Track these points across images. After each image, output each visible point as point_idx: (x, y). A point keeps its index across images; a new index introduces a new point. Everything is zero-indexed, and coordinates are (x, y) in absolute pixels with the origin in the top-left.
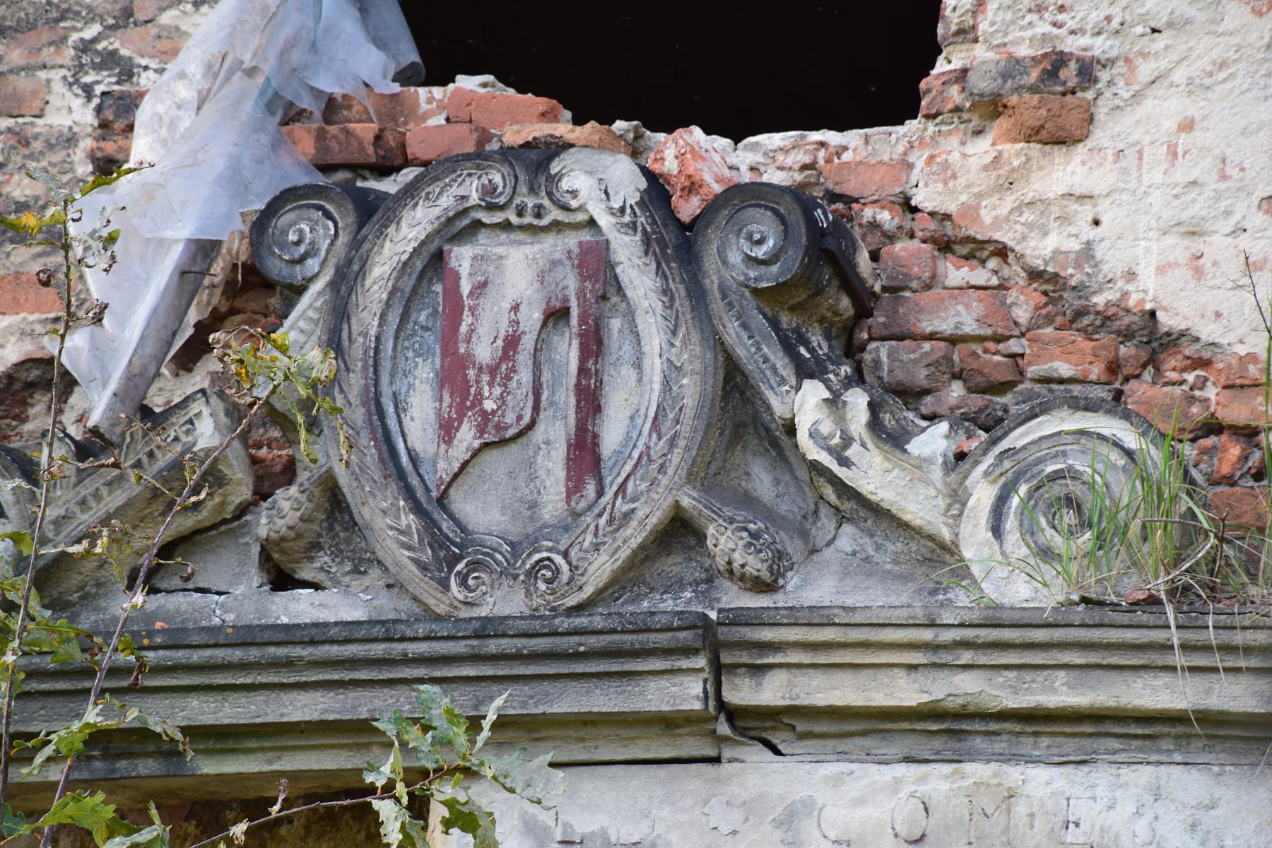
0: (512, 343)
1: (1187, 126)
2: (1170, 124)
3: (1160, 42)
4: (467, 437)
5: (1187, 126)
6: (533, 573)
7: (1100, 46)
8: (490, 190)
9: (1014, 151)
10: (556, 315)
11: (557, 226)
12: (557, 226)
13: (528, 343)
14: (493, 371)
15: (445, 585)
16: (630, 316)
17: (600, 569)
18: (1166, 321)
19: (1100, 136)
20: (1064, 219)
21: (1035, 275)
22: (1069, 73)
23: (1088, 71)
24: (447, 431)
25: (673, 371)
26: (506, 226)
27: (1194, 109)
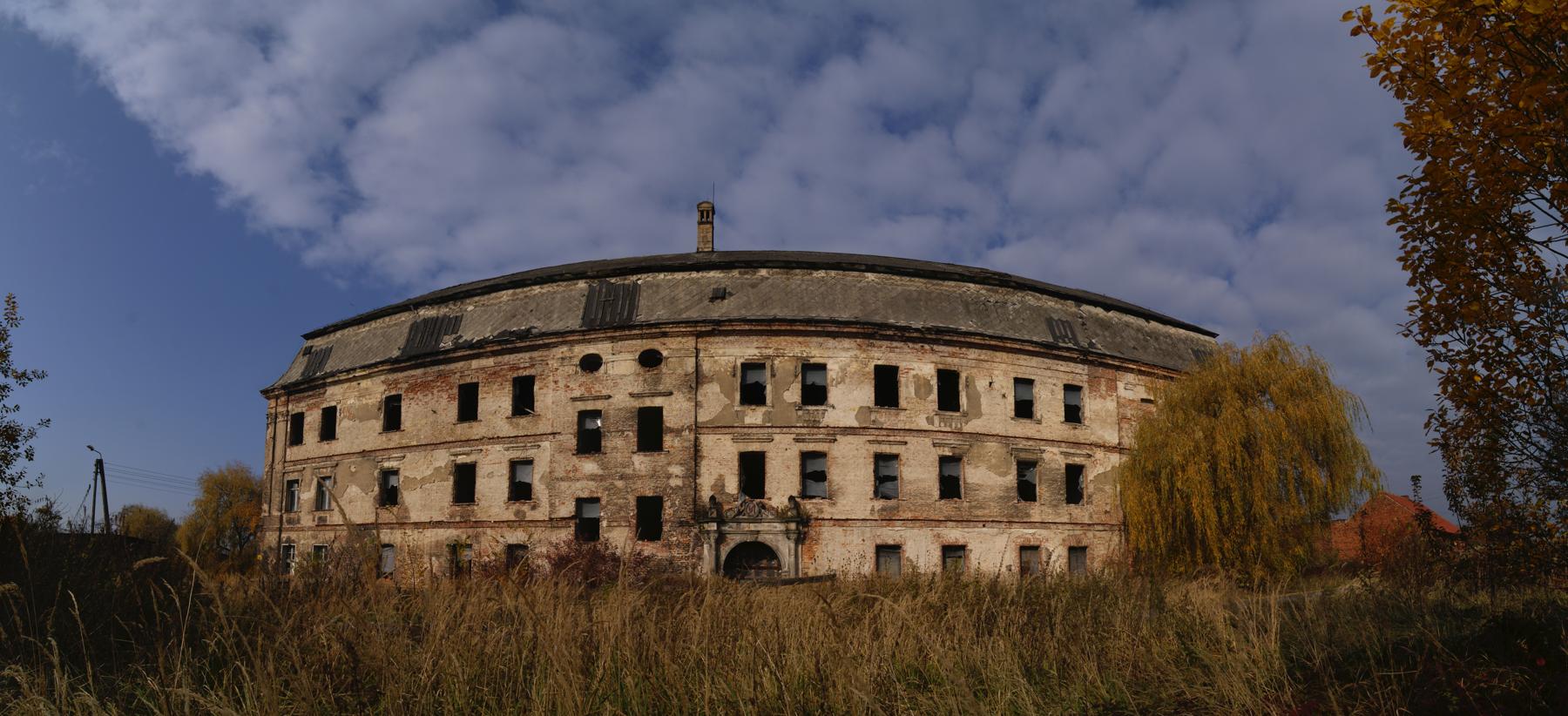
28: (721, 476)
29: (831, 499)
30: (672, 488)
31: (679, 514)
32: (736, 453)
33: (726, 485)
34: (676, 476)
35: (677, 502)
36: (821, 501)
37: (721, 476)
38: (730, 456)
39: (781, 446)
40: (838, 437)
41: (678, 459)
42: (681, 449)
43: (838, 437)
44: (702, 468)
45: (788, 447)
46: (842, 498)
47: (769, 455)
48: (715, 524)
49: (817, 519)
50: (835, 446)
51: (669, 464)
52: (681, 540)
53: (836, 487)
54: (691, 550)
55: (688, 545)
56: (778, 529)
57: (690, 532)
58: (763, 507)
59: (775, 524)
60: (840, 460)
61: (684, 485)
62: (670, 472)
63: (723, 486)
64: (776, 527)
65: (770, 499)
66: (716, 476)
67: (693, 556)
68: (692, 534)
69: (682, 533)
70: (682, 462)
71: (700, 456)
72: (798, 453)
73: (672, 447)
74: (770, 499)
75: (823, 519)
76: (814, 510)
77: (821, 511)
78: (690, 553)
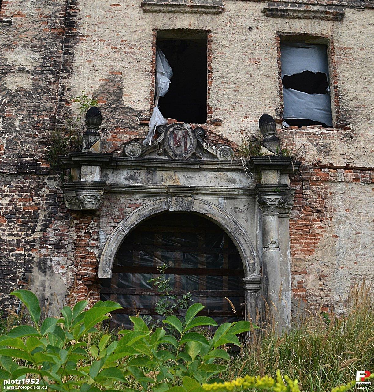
0: (180, 138)
1: (228, 125)
2: (227, 125)
3: (226, 119)
4: (176, 146)
5: (228, 125)
6: (183, 157)
7: (222, 119)
8: (178, 126)
9: (215, 126)
10: (183, 137)
11: (183, 130)
12: (183, 130)
13: (181, 138)
14: (178, 140)
15: (175, 157)
16: (190, 137)
17: (188, 156)
18: (228, 140)
19: (222, 126)
20: (220, 132)
21: (218, 136)
22: (220, 121)
23: (221, 120)
24: (174, 145)
25: (193, 141)
26: (179, 129)
27: (229, 124)
28: (115, 73)
29: (343, 126)
30: (9, 93)
31: (19, 148)
32: (149, 31)
33: (125, 91)
34: (22, 70)
35: (17, 123)
36: (324, 130)
37: (115, 73)
38: (136, 37)
39: (240, 22)
40: (348, 12)
41: (28, 36)
42: (36, 18)
43: (348, 12)
44: (77, 57)
45: (253, 25)
46: (366, 124)
47: (217, 37)
48: (98, 169)
49: (318, 166)
50: (342, 28)
51: (8, 46)
52: (20, 204)
53: (351, 104)
54: (38, 228)
55: (36, 216)
56: (238, 185)
57: (40, 187)
58: (204, 136)
59: (231, 175)
60: (357, 53)
61: (35, 89)
62: (9, 62)
63: (119, 93)
64: (234, 181)
65: (217, 123)
66: (105, 73)
67: (44, 241)
68: (45, 192)
69: (22, 190)
70: (36, 42)
71: (75, 36)
72: (272, 36)
73: (19, 14)
74: (217, 123)
75: (331, 167)
76: (313, 150)
77: (324, 150)
78: (38, 235)
